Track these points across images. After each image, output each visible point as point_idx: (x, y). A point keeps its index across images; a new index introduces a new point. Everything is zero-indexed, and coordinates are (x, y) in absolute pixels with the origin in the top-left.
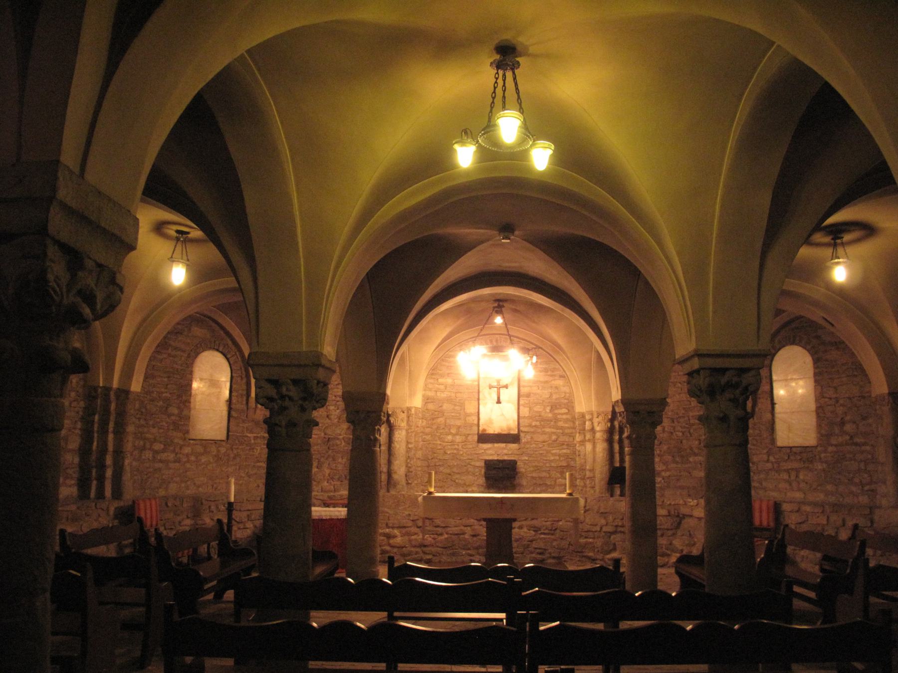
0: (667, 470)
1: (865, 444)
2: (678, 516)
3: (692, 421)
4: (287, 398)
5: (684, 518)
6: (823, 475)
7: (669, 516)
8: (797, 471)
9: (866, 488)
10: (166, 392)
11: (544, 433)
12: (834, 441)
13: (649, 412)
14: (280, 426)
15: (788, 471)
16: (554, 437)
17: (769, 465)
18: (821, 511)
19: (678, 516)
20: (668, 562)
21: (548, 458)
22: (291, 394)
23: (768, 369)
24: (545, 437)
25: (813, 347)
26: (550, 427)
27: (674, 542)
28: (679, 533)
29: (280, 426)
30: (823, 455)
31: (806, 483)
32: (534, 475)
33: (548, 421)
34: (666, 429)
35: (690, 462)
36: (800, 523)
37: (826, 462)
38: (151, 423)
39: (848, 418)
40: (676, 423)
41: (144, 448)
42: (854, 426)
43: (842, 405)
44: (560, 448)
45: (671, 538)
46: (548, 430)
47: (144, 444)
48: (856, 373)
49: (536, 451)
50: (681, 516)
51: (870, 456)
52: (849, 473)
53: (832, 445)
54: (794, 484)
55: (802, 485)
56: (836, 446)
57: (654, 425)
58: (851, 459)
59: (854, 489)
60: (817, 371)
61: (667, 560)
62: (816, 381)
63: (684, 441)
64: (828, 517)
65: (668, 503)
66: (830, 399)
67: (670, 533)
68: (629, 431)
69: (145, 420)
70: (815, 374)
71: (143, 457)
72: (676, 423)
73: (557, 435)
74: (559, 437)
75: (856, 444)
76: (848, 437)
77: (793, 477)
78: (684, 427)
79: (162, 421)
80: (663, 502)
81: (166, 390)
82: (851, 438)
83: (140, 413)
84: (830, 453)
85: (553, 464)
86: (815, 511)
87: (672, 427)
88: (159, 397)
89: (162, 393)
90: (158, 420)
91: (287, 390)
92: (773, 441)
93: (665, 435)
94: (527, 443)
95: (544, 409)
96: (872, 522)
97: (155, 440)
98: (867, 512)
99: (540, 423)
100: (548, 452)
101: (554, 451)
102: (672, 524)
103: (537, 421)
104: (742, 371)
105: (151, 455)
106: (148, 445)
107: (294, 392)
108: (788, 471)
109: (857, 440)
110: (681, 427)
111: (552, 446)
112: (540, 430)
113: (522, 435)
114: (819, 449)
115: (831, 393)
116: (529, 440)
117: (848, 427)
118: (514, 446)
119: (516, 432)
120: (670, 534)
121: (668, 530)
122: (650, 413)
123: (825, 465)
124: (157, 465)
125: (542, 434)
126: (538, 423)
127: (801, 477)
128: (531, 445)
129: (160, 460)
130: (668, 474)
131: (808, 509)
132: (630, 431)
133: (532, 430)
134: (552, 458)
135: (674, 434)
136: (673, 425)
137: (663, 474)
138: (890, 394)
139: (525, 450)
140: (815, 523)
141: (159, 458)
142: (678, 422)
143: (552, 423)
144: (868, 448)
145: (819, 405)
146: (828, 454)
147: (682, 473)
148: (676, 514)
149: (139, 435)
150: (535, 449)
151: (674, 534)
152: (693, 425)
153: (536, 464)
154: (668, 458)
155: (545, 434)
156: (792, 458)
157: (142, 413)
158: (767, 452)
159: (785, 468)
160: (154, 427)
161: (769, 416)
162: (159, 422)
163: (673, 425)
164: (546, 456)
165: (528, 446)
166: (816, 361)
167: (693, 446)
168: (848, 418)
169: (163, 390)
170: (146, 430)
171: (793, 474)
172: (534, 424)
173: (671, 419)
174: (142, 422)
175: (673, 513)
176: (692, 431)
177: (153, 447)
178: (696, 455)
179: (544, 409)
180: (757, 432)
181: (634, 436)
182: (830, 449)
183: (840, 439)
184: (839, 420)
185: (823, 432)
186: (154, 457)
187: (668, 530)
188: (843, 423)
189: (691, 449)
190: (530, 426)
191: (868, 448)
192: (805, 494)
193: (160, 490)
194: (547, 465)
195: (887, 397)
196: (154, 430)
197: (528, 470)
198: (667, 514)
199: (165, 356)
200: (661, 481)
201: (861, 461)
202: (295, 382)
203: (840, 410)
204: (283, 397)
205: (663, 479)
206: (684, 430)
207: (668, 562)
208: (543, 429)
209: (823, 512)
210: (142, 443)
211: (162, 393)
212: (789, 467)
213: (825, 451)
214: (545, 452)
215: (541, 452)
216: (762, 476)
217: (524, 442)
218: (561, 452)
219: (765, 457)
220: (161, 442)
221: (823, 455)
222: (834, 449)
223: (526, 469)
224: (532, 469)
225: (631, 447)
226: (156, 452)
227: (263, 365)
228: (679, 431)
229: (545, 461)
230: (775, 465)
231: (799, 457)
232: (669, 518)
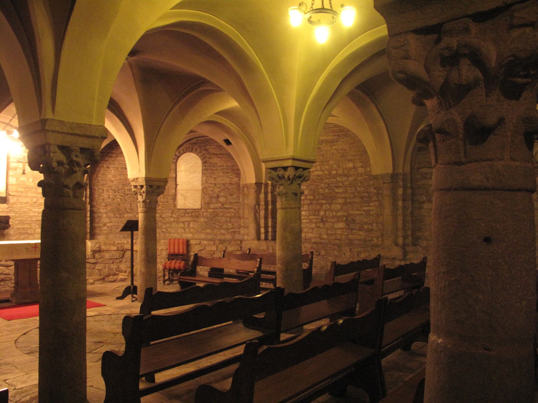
0: (111, 222)
1: (231, 208)
2: (123, 250)
3: (126, 193)
5: (126, 251)
6: (204, 224)
7: (118, 250)
8: (189, 222)
9: (231, 231)
11: (27, 197)
12: (212, 206)
13: (157, 186)
14: (69, 188)
15: (183, 222)
16: (35, 200)
17: (172, 219)
18: (213, 243)
19: (123, 250)
20: (117, 279)
21: (30, 215)
23: (175, 164)
24: (28, 200)
25: (203, 155)
26: (32, 193)
27: (120, 266)
28: (124, 260)
29: (69, 188)
30: (205, 214)
31: (194, 229)
32: (19, 226)
33: (31, 188)
34: (111, 197)
35: (125, 217)
36: (200, 251)
37: (207, 218)
39: (222, 194)
40: (117, 193)
42: (225, 199)
43: (219, 188)
44: (39, 207)
45: (119, 264)
46: (30, 195)
48: (228, 171)
49: (20, 209)
50: (125, 250)
51: (233, 215)
52: (220, 223)
53: (210, 208)
54: (187, 230)
55: (192, 230)
56: (213, 209)
57: (159, 195)
58: (221, 216)
59: (223, 231)
60: (204, 168)
61: (116, 278)
62: (203, 173)
63: (121, 204)
64: (217, 247)
65: (117, 242)
66: (211, 184)
67: (118, 261)
68: (144, 197)
70: (203, 170)
72: (117, 193)
73: (37, 198)
74: (38, 200)
75: (225, 208)
76: (221, 205)
77: (186, 226)
78: (122, 196)
80: (114, 242)
82: (223, 205)
84: (209, 213)
85: (33, 219)
86: (210, 243)
87: (114, 195)
92: (175, 205)
93: (110, 200)
94: (14, 203)
95: (28, 180)
96: (241, 248)
98: (239, 242)
99: (24, 189)
100: (29, 210)
101: (34, 210)
102: (119, 256)
103: (22, 188)
104: (304, 169)
108: (183, 222)
109: (226, 206)
110: (120, 195)
111: (33, 206)
112: (24, 195)
113: (10, 197)
114: (203, 210)
115: (212, 181)
116: (16, 201)
117: (222, 199)
118: (4, 206)
119: (4, 195)
120: (118, 262)
121: (117, 259)
122: (158, 187)
123: (206, 220)
125: (25, 197)
126: (23, 190)
127: (191, 226)
128: (17, 205)
130: (111, 224)
131: (206, 242)
132: (146, 198)
133: (18, 194)
134: (33, 214)
135: (115, 200)
136: (115, 194)
137: (108, 225)
138: (256, 183)
139: (12, 209)
140: (210, 250)
142: (119, 193)
143: (34, 190)
144: (233, 210)
145: (204, 187)
146: (208, 213)
147: (120, 224)
148: (122, 249)
150: (20, 208)
151: (121, 261)
152: (127, 194)
153: (21, 219)
154: (111, 215)
155: (28, 197)
156: (186, 215)
158: (172, 212)
159: (182, 221)
161: (174, 191)
163: (115, 194)
164: (28, 213)
165: (14, 206)
166: (204, 163)
167: (126, 208)
168: (222, 194)
171: (187, 224)
172: (20, 190)
173: (114, 190)
175: (120, 248)
176: (126, 198)
178: (128, 213)
179: (28, 180)
180: (166, 200)
181: (148, 201)
182: (210, 210)
183: (216, 205)
184: (216, 195)
185: (206, 201)
187: (117, 259)
188: (218, 197)
189: (125, 209)
190: (16, 191)
191: (233, 210)
192: (193, 234)
194: (29, 219)
195: (254, 185)
197: (15, 223)
198: (117, 249)
200: (106, 229)
201: (228, 217)
203: (217, 190)
205: (108, 228)
206: (121, 197)
207: (117, 279)
208: (26, 194)
209: (214, 244)
212: (184, 220)
213: (207, 212)
214: (27, 210)
215: (24, 210)
216: (168, 225)
217: (12, 203)
218: (39, 211)
219: (170, 215)
221: (205, 214)
222: (212, 210)
223: (13, 223)
224: (17, 222)
225: (146, 208)
228: (118, 198)
229: (27, 217)
230: (176, 219)
231: (190, 215)
232: (117, 252)
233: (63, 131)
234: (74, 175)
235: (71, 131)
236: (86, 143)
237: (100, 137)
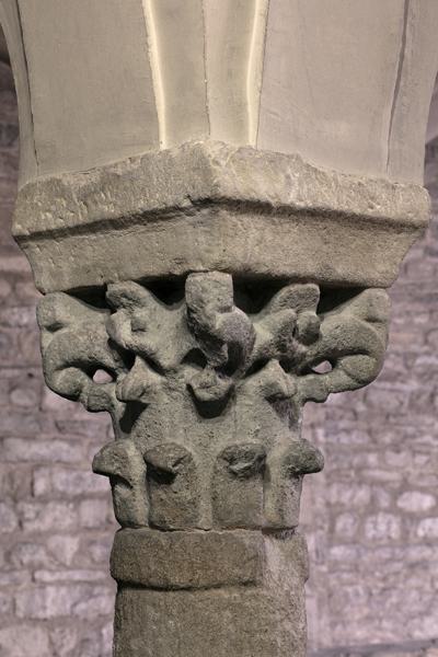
4: (139, 361)
10: (428, 354)
22: (148, 341)
38: (388, 438)
41: (372, 508)
47: (373, 499)
69: (369, 432)
71: (370, 533)
79: (422, 433)
81: (426, 348)
83: (350, 415)
88: (408, 367)
89: (415, 355)
90: (410, 430)
91: (138, 329)
97: (406, 486)
105: (395, 527)
106: (384, 502)
107: (161, 331)
124: (415, 554)
129: (425, 538)
141: (421, 533)
149: (352, 473)
157: (355, 414)
160: (398, 452)
162: (414, 437)
169: (415, 348)
170: (372, 459)
174: (359, 439)
177: (400, 504)
186: (405, 533)
193: (428, 621)
196: (394, 459)
199: (418, 253)
202: (168, 289)
204: (127, 357)
210: (363, 494)
211: (415, 355)
220: (423, 490)
226: (413, 518)
227: (51, 235)
233: (60, 223)
234: (145, 414)
235: (82, 217)
236: (152, 252)
237: (186, 203)
